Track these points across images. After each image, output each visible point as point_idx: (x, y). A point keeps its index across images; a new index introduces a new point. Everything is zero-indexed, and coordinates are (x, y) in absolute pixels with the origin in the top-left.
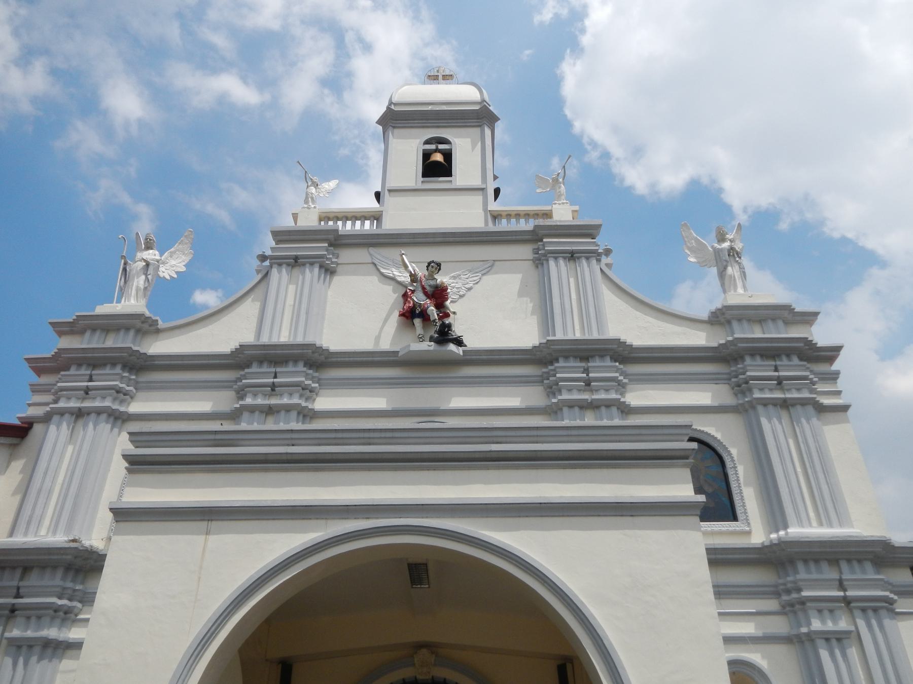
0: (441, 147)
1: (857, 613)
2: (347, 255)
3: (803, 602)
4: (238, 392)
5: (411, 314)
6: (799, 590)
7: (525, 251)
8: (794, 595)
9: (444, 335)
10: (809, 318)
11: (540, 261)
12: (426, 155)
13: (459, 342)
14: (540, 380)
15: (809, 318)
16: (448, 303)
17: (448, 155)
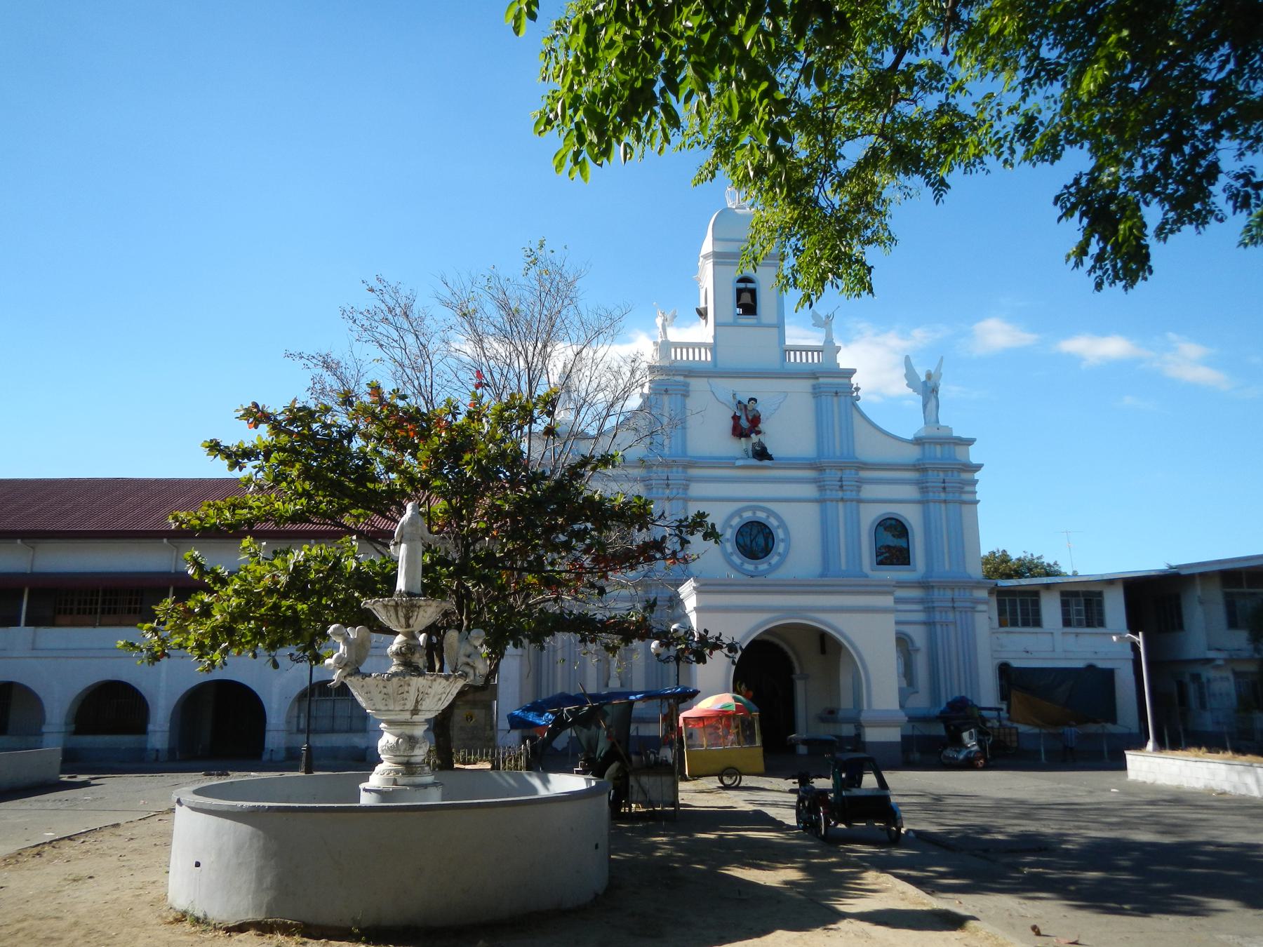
0: (750, 285)
1: (957, 613)
2: (697, 384)
3: (934, 608)
4: (645, 486)
5: (739, 432)
6: (933, 602)
7: (806, 385)
8: (930, 605)
9: (762, 454)
10: (970, 442)
11: (817, 393)
12: (739, 292)
13: (770, 458)
14: (814, 481)
15: (970, 442)
16: (760, 425)
17: (753, 293)
